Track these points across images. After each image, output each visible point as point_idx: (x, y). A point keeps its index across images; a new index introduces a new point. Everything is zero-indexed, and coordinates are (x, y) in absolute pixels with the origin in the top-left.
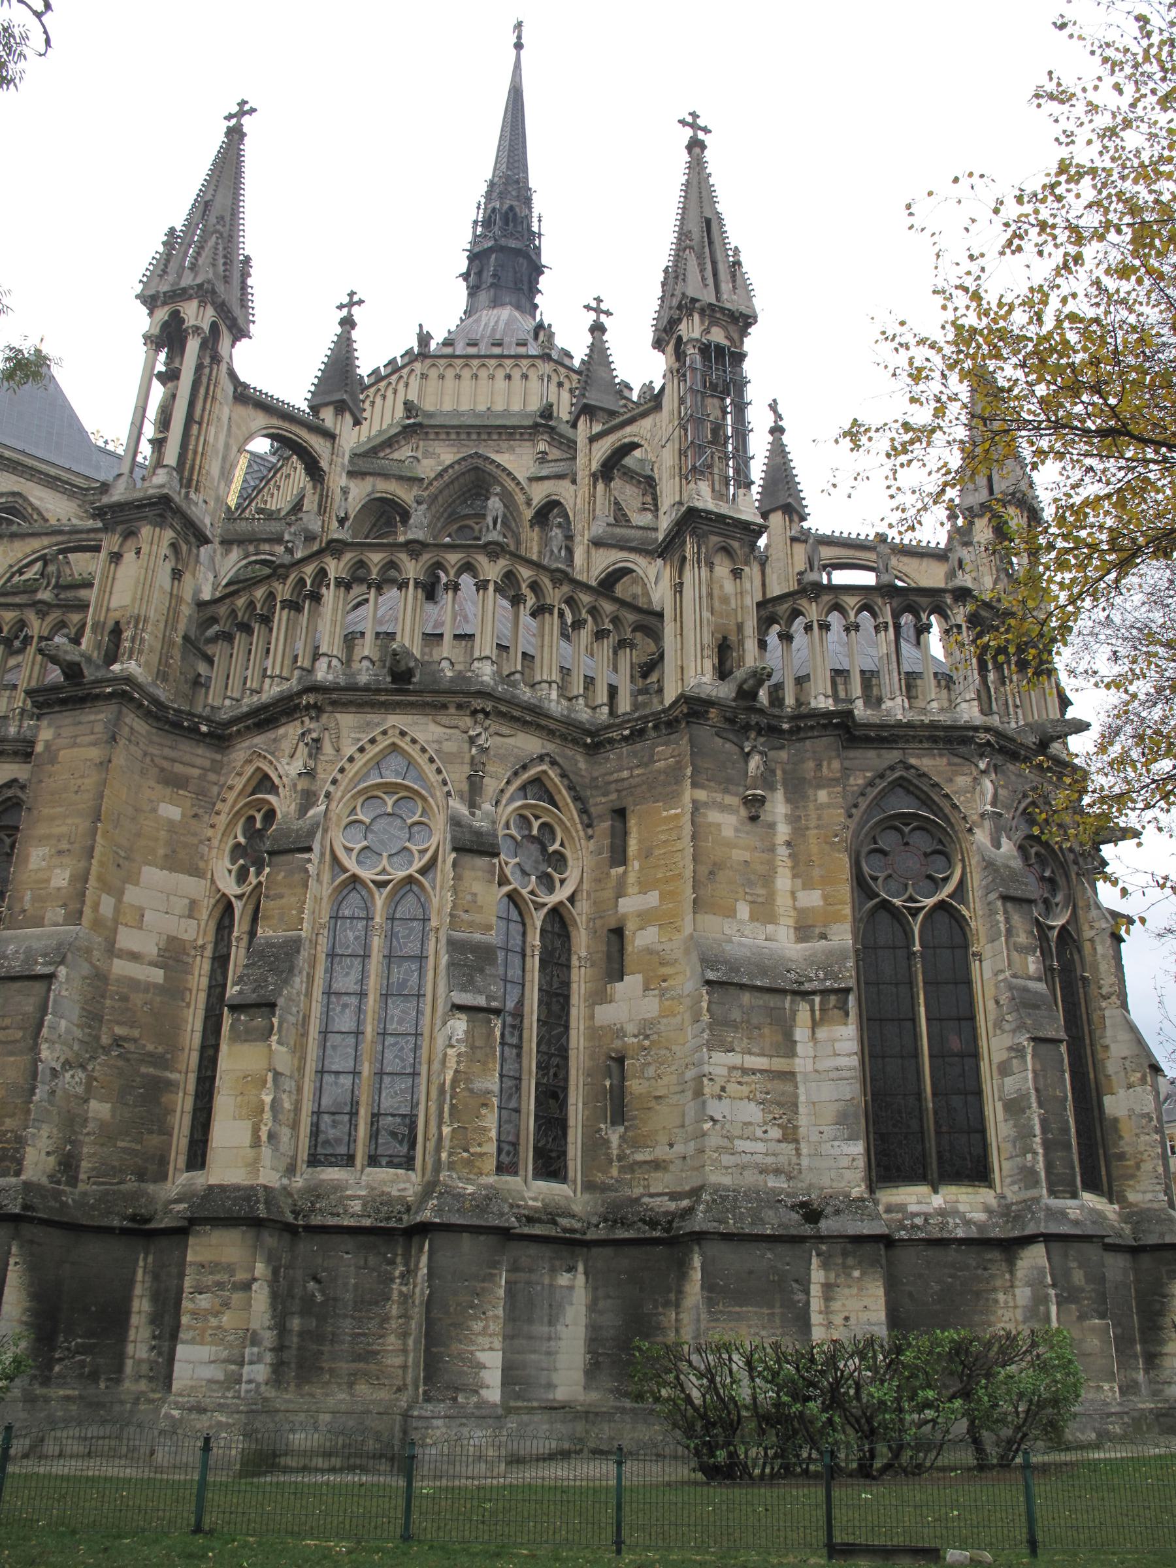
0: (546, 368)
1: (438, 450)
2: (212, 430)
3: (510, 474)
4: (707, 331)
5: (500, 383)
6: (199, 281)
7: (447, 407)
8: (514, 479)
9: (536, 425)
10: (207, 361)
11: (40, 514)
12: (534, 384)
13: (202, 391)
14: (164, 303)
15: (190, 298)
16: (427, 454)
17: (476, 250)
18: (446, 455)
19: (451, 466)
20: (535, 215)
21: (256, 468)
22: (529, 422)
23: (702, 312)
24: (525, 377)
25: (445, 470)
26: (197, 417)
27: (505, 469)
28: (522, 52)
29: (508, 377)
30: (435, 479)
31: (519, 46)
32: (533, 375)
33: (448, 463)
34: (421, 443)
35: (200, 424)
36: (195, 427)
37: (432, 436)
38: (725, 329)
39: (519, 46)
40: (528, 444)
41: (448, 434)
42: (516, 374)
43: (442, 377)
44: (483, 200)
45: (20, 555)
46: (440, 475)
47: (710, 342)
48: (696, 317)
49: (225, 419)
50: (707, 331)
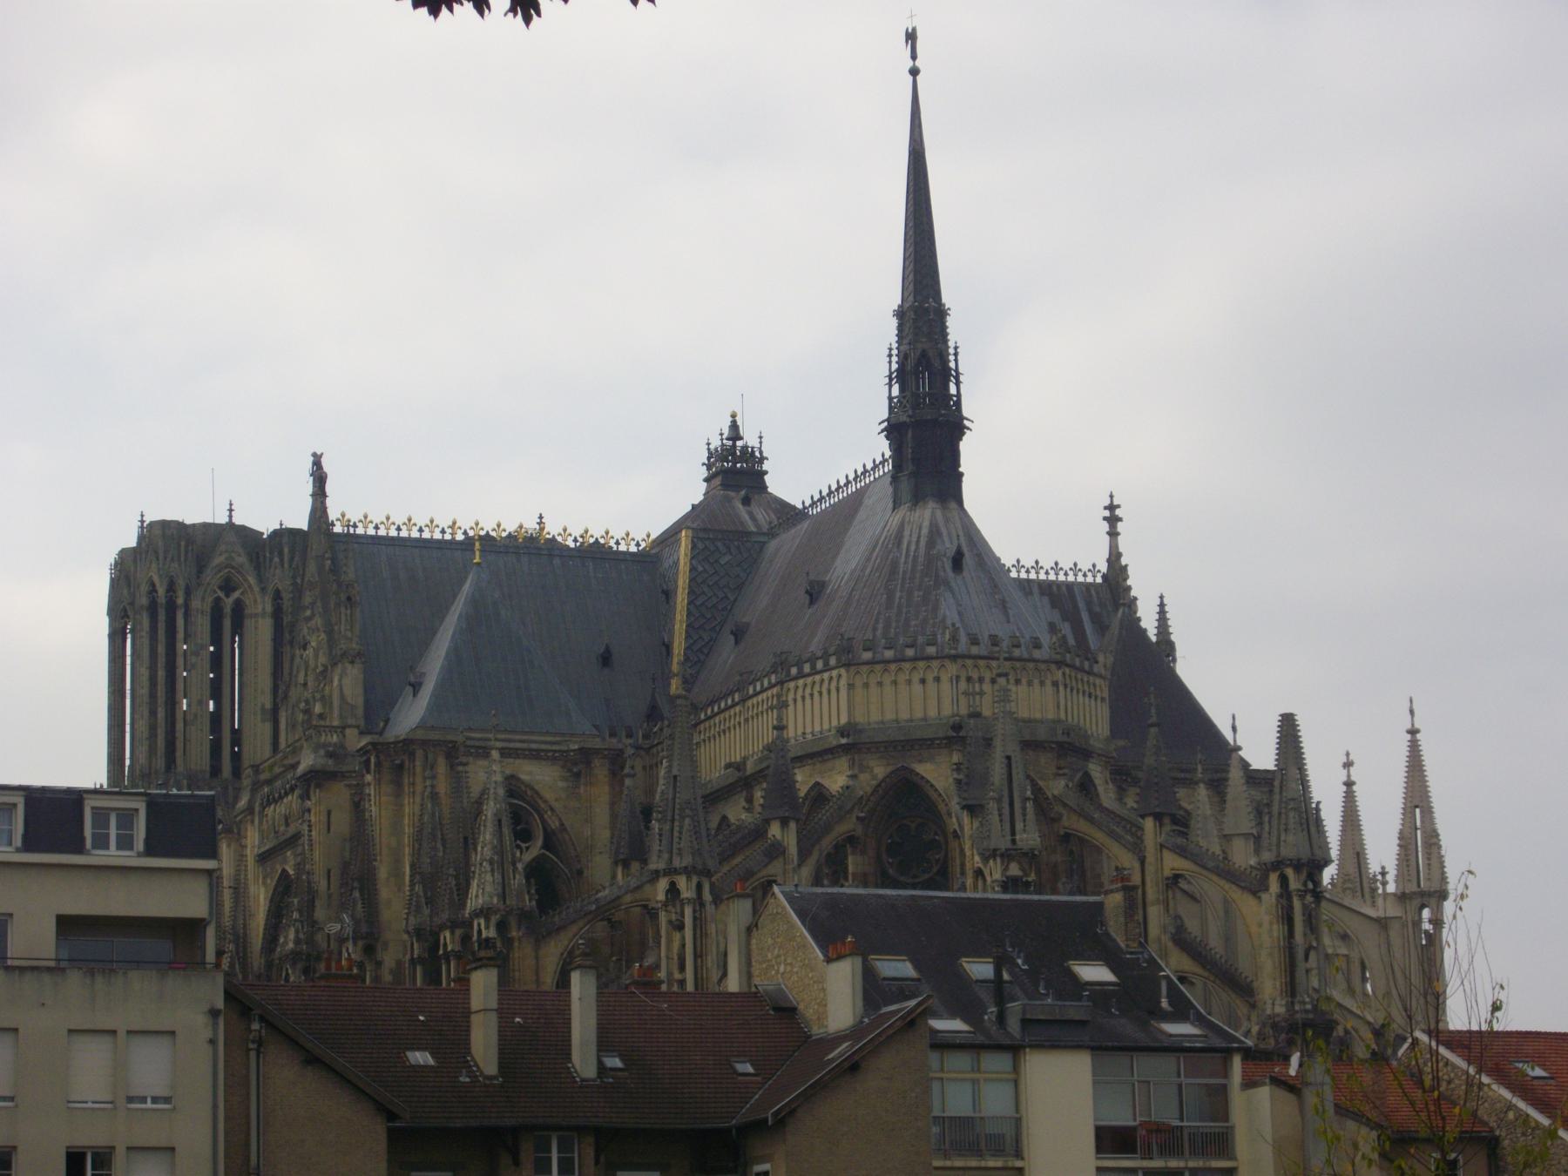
0: (952, 668)
1: (872, 763)
2: (709, 958)
3: (932, 786)
4: (1006, 869)
5: (917, 688)
6: (683, 865)
7: (875, 717)
8: (936, 790)
10: (698, 908)
11: (532, 789)
12: (945, 686)
13: (698, 932)
14: (665, 875)
15: (680, 874)
16: (863, 768)
18: (880, 770)
19: (883, 781)
20: (951, 344)
21: (700, 545)
22: (941, 735)
23: (1002, 856)
24: (937, 679)
25: (879, 785)
26: (699, 953)
27: (928, 781)
28: (919, 78)
29: (923, 681)
30: (872, 794)
31: (914, 72)
32: (945, 678)
33: (880, 777)
34: (856, 757)
35: (701, 957)
36: (699, 960)
38: (1019, 863)
39: (914, 72)
42: (930, 677)
43: (866, 685)
44: (895, 345)
45: (566, 943)
46: (875, 790)
47: (1007, 877)
48: (998, 860)
49: (714, 931)
50: (1006, 869)
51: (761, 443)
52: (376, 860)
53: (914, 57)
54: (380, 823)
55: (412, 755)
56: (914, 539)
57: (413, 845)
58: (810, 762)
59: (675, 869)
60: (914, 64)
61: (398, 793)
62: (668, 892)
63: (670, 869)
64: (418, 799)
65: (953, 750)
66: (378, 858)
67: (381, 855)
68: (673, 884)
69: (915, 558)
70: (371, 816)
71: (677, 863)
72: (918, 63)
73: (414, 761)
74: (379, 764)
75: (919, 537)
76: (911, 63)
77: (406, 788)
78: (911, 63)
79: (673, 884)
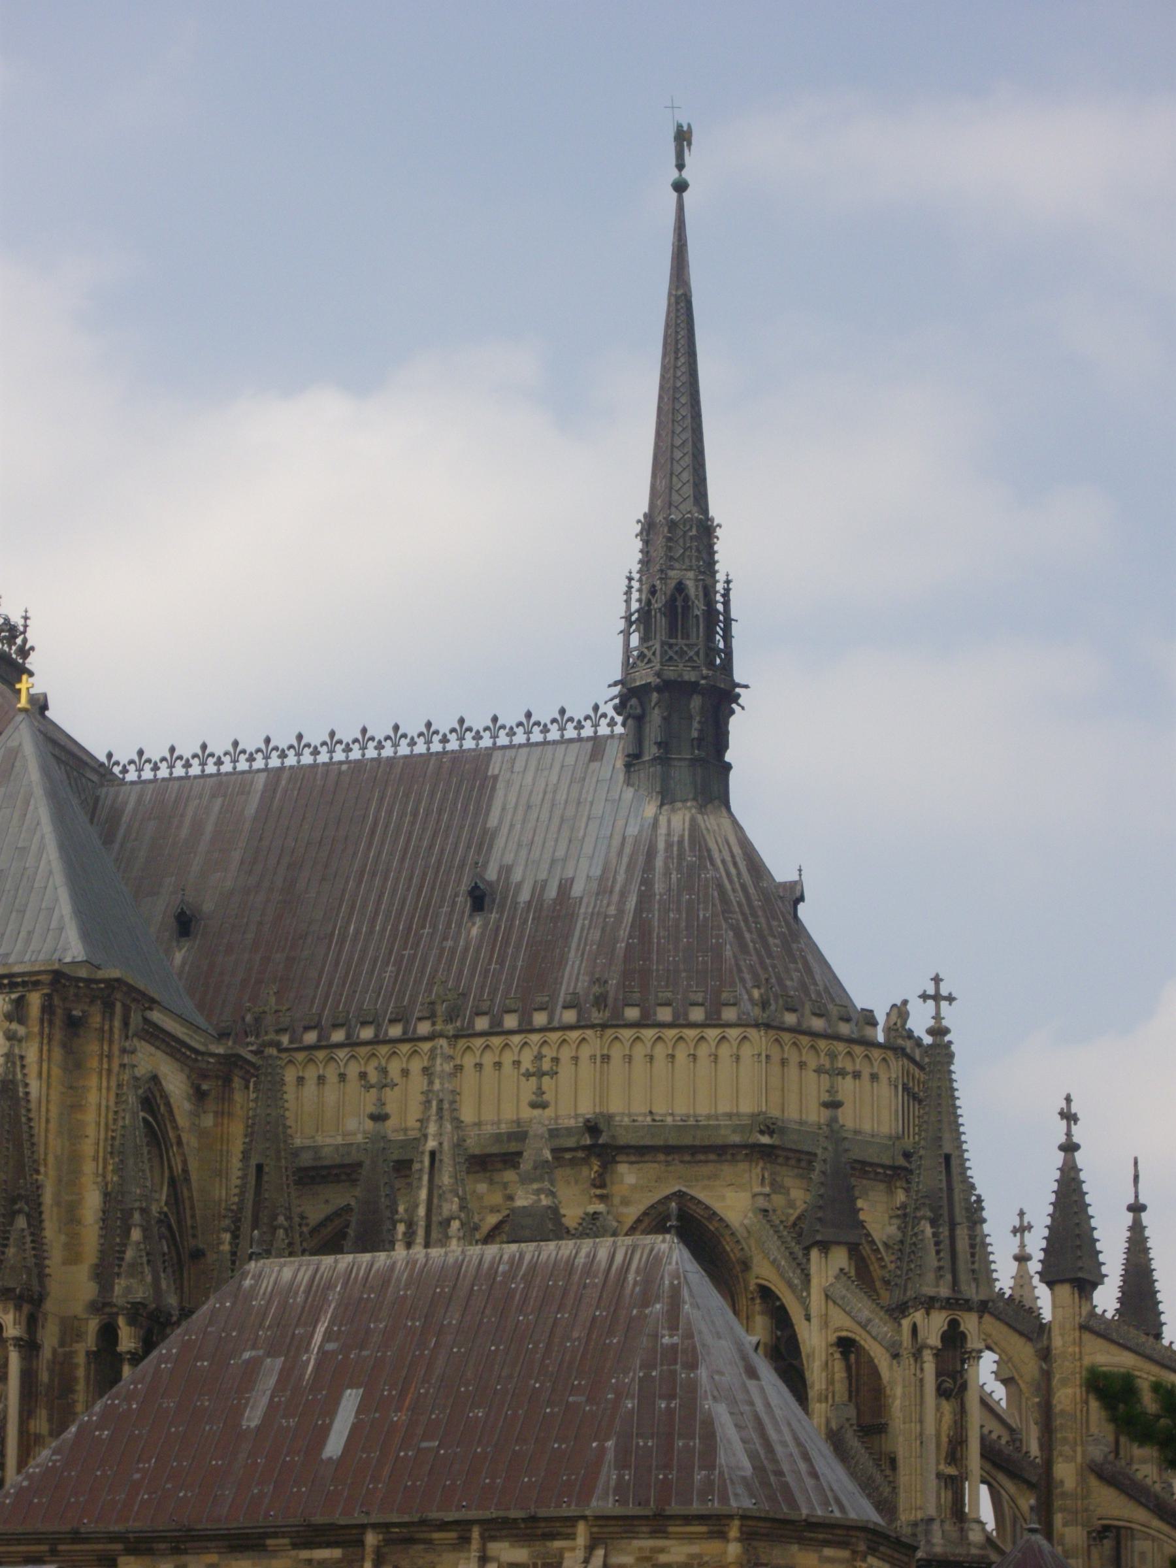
0: (897, 1066)
1: (788, 1182)
9: (895, 1168)
12: (884, 1090)
14: (942, 1308)
15: (970, 1309)
17: (670, 673)
24: (874, 1077)
31: (680, 187)
37: (780, 1160)
39: (680, 187)
40: (882, 1186)
41: (799, 1160)
42: (866, 1075)
51: (26, 626)
52: (38, 1172)
53: (680, 166)
54: (48, 1110)
55: (109, 1006)
56: (728, 859)
57: (105, 1159)
58: (661, 1157)
59: (967, 1301)
60: (681, 175)
61: (74, 1064)
62: (945, 1337)
63: (957, 1300)
64: (113, 1084)
65: (896, 1188)
66: (42, 1169)
67: (46, 1165)
68: (954, 1324)
69: (744, 887)
70: (27, 1094)
71: (970, 1291)
72: (686, 174)
73: (111, 1020)
74: (47, 1009)
75: (733, 856)
76: (674, 174)
77: (94, 1063)
78: (674, 174)
79: (954, 1324)
